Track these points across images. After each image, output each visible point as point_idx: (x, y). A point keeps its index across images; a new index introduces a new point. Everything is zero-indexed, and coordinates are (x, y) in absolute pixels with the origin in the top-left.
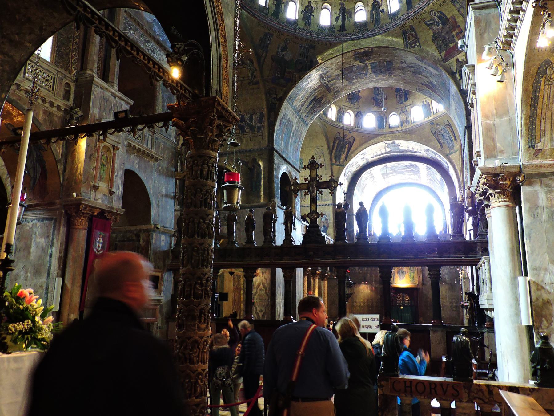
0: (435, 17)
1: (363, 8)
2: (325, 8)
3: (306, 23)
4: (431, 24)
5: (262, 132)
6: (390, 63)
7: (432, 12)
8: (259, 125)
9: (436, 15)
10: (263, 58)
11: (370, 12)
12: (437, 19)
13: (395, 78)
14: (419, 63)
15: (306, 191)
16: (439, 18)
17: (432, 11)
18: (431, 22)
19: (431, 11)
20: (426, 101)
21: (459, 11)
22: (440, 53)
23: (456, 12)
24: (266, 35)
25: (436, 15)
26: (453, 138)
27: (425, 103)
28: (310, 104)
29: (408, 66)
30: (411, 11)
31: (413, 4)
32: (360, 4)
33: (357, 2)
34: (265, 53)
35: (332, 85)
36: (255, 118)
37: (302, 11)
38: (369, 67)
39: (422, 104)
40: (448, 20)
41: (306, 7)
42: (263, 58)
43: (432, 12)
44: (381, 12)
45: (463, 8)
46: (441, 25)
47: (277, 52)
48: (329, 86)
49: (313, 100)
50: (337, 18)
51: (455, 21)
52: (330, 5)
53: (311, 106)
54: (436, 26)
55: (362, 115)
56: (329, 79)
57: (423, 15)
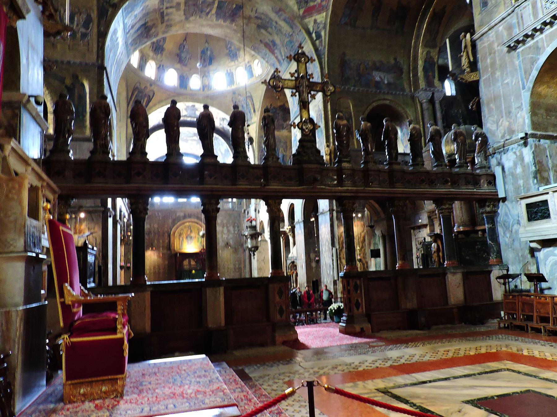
5: (88, 41)
6: (240, 7)
8: (83, 30)
13: (235, 27)
14: (273, 15)
15: (294, 91)
20: (230, 70)
22: (299, 9)
26: (252, 111)
27: (229, 71)
28: (138, 30)
29: (256, 17)
35: (167, 14)
36: (78, 20)
38: (216, 5)
39: (226, 72)
48: (165, 14)
49: (142, 25)
53: (139, 32)
55: (164, 70)
56: (168, 5)
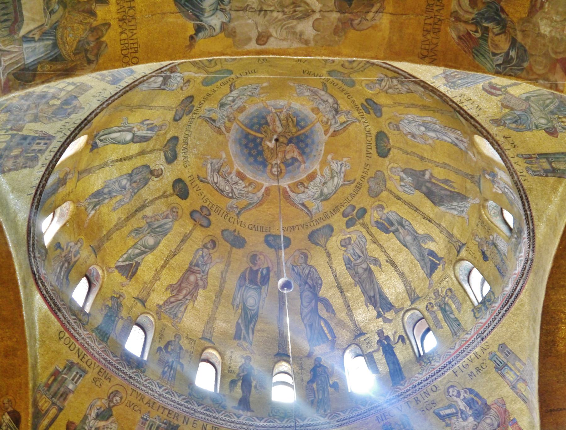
0: (458, 399)
1: (288, 379)
2: (207, 361)
3: (164, 373)
4: (449, 416)
7: (451, 390)
9: (462, 397)
10: (45, 422)
11: (305, 384)
12: (462, 405)
16: (470, 403)
17: (452, 387)
18: (448, 411)
19: (449, 388)
21: (513, 388)
23: (506, 392)
24: (70, 366)
25: (462, 397)
30: (402, 387)
31: (406, 374)
32: (284, 366)
33: (279, 361)
34: (54, 411)
37: (160, 349)
40: (489, 408)
41: (168, 343)
42: (45, 422)
43: (451, 390)
44: (331, 386)
45: (524, 381)
46: (471, 419)
47: (86, 417)
50: (233, 383)
51: (505, 411)
52: (220, 354)
54: (460, 420)
57: (431, 394)
